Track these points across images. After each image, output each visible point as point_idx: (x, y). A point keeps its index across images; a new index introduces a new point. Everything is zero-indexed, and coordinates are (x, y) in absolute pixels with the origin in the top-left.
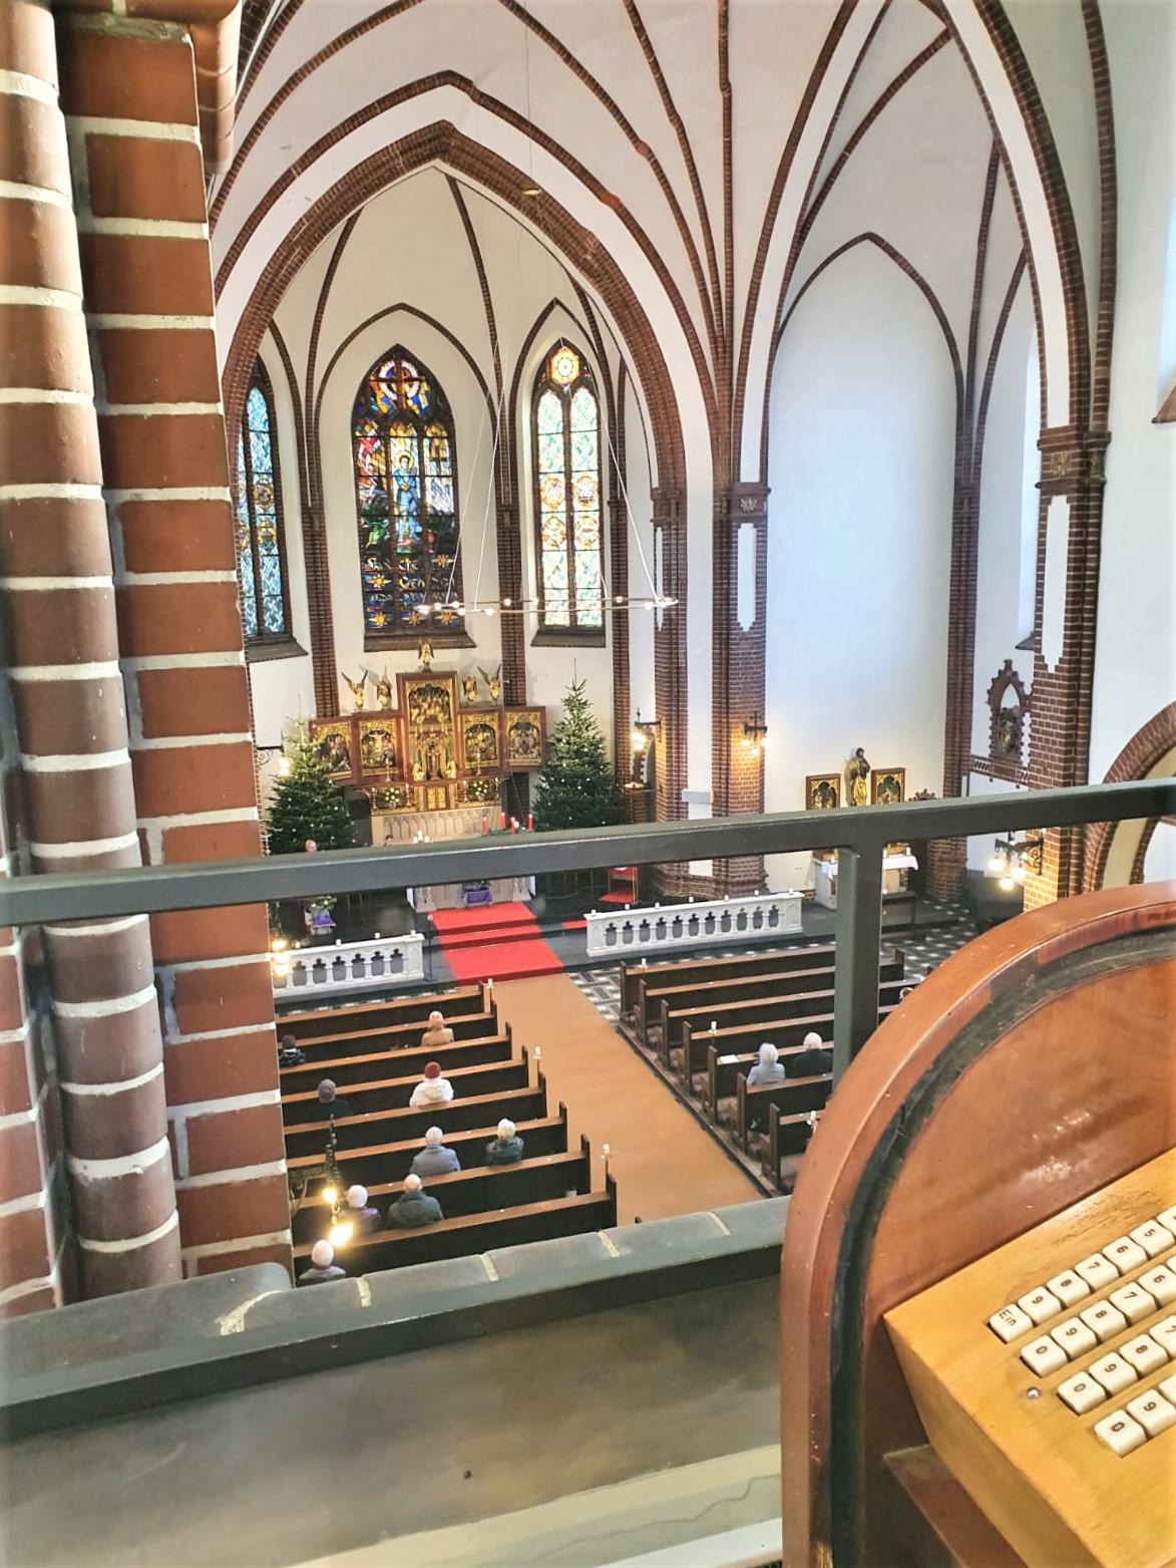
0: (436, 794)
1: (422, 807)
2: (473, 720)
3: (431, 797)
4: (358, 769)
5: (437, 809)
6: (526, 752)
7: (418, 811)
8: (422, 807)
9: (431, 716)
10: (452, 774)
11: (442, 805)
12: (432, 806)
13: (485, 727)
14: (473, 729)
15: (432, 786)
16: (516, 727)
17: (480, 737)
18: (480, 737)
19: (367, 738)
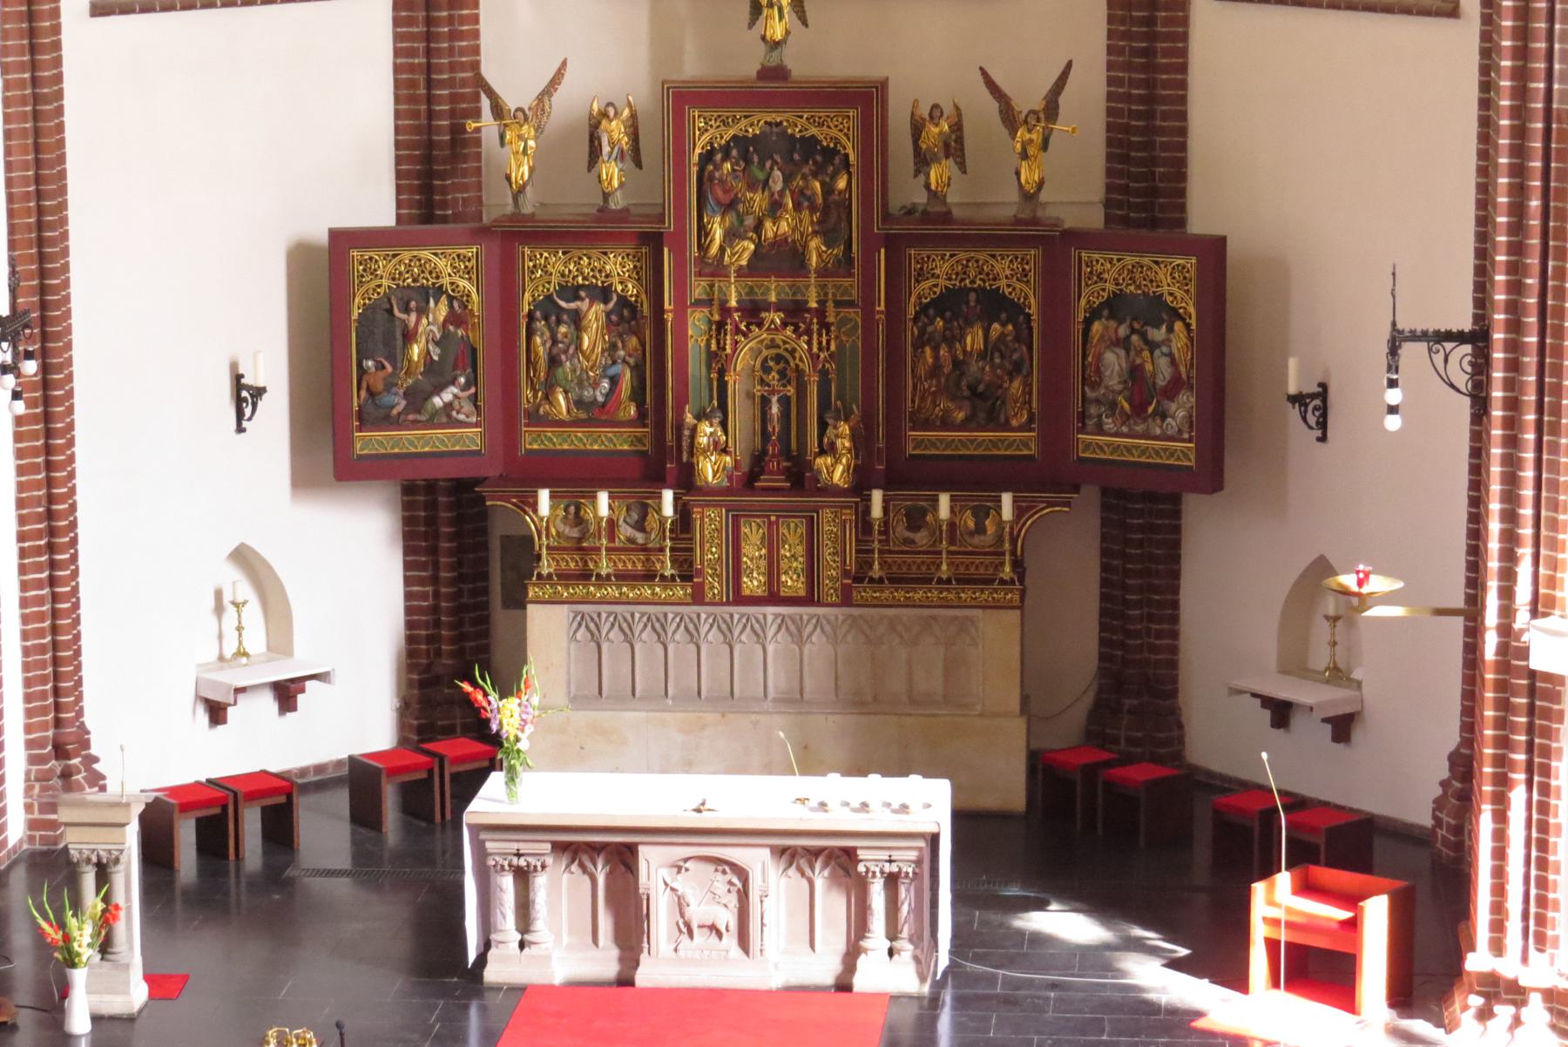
0: (772, 544)
1: (715, 586)
2: (942, 270)
3: (753, 551)
4: (507, 417)
5: (773, 597)
6: (1139, 409)
7: (698, 598)
8: (715, 586)
9: (780, 242)
10: (837, 472)
11: (792, 582)
12: (753, 583)
13: (995, 305)
14: (949, 303)
15: (763, 512)
16: (1114, 306)
17: (974, 339)
18: (974, 339)
19: (548, 308)
